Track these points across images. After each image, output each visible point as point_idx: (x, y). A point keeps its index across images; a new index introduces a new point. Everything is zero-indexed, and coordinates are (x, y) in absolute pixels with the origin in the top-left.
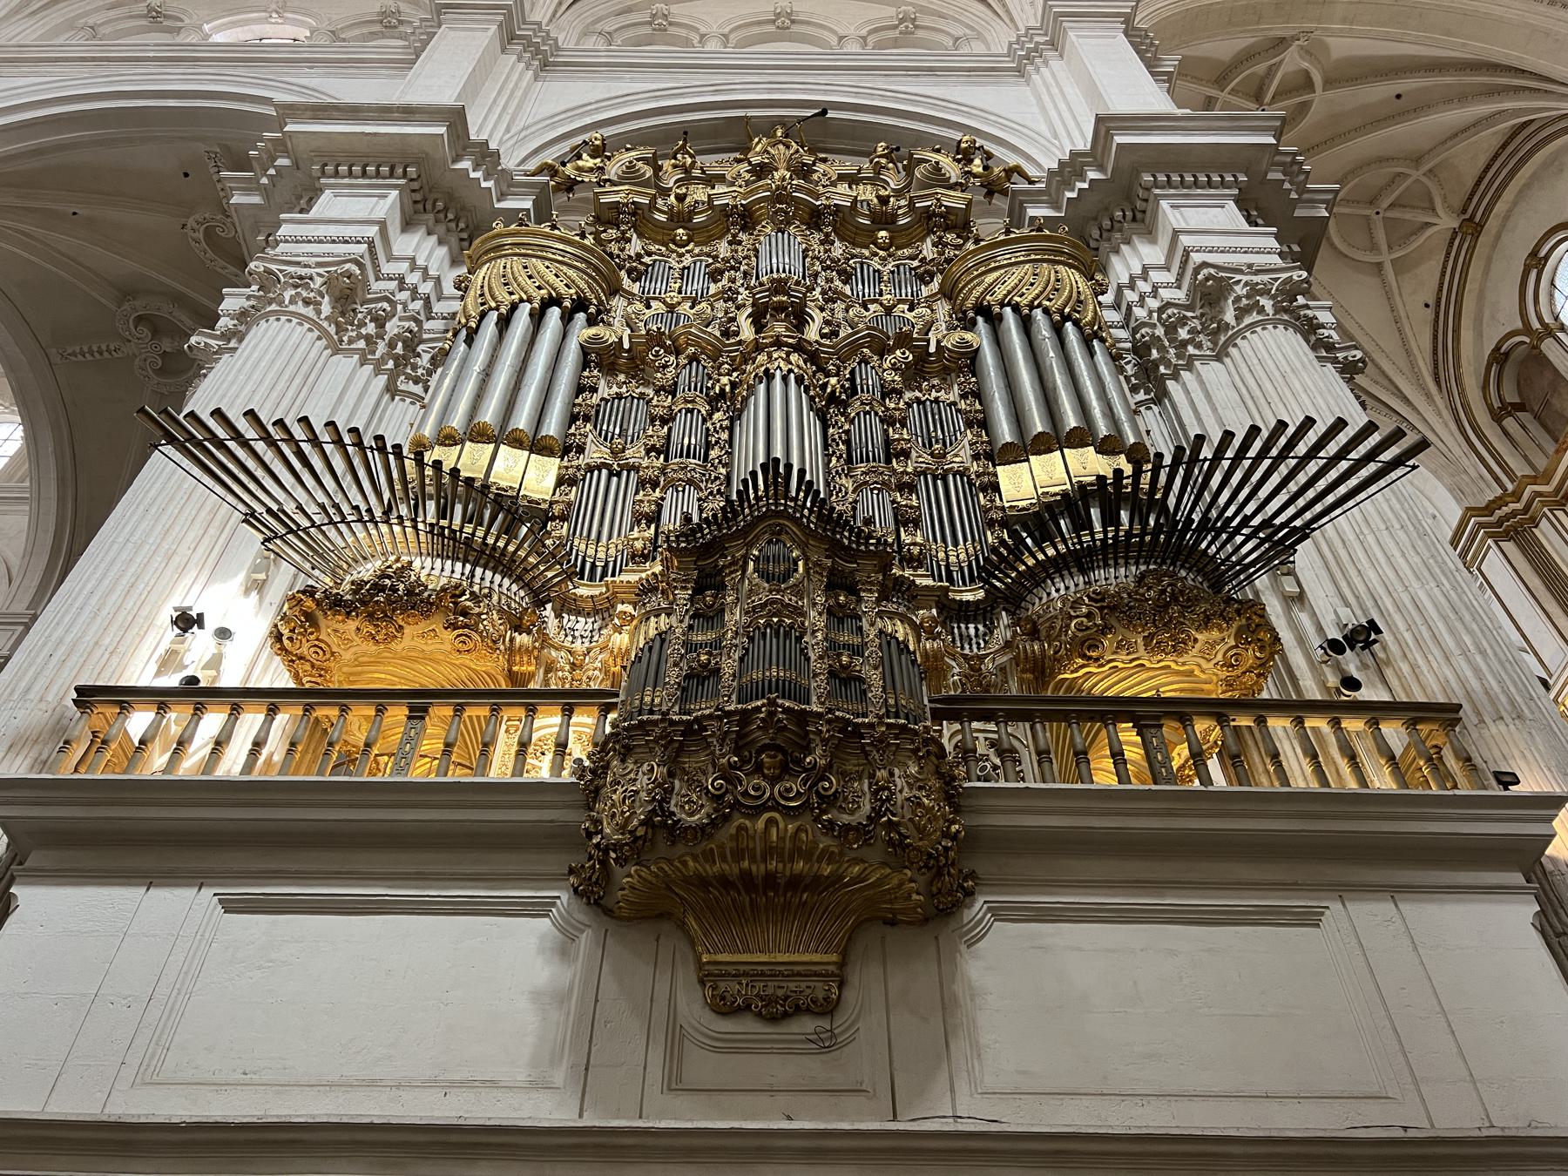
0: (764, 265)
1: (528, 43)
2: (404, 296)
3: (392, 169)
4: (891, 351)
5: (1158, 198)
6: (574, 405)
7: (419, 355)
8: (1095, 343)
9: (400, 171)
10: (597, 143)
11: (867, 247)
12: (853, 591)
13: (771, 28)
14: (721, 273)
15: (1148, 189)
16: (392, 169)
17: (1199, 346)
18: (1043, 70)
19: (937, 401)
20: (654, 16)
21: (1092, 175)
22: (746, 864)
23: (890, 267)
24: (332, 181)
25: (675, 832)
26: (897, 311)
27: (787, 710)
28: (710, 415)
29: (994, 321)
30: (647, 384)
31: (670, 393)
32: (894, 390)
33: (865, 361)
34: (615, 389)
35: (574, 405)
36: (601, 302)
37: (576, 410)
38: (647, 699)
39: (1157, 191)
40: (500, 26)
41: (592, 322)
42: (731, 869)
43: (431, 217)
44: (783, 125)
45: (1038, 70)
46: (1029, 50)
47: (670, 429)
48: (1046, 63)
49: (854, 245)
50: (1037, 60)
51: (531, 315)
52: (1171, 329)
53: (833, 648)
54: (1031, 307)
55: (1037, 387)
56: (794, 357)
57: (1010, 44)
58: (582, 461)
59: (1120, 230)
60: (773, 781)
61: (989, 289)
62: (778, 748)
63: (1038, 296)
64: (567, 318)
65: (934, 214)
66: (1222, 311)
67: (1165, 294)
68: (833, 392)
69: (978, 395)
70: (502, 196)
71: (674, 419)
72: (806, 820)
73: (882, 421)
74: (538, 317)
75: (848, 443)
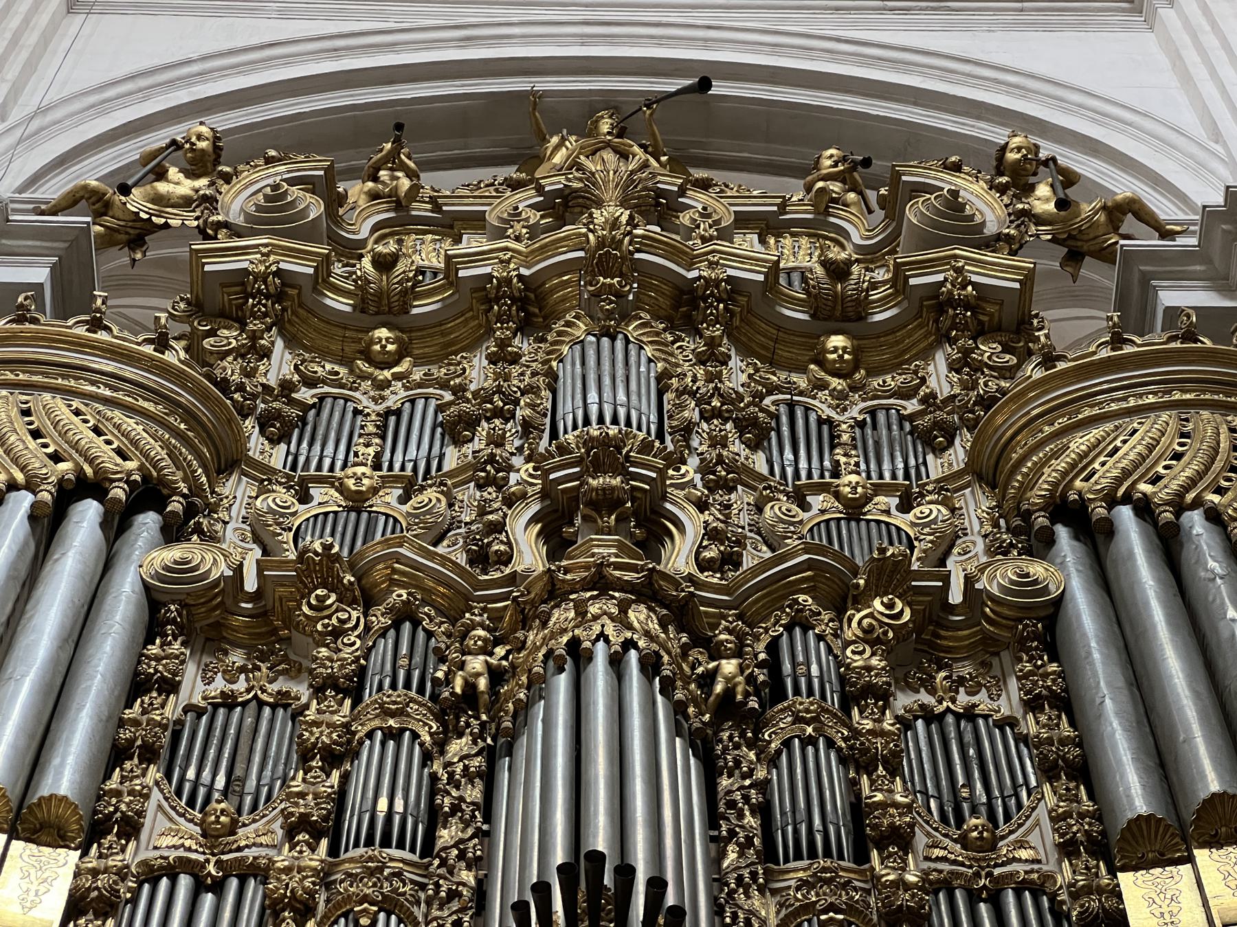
0: (568, 408)
4: (860, 599)
6: (122, 723)
10: (203, 145)
11: (803, 370)
14: (471, 423)
19: (970, 714)
23: (854, 412)
26: (872, 512)
28: (441, 745)
30: (294, 671)
31: (346, 692)
32: (870, 690)
34: (219, 684)
35: (122, 723)
36: (196, 489)
37: (125, 734)
41: (172, 533)
47: (345, 778)
49: (774, 363)
51: (33, 518)
54: (1179, 506)
55: (1203, 688)
56: (638, 615)
58: (132, 855)
61: (1081, 466)
63: (1193, 482)
65: (951, 302)
68: (729, 692)
71: (356, 755)
73: (842, 761)
75: (764, 811)
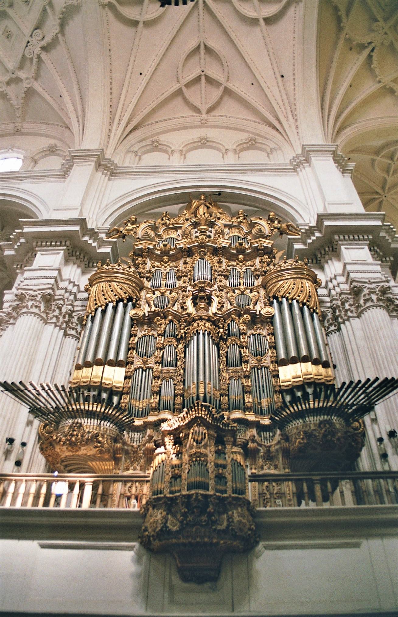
0: (196, 274)
1: (106, 167)
2: (67, 295)
3: (61, 243)
4: (242, 316)
6: (129, 344)
7: (73, 317)
8: (315, 314)
9: (63, 244)
10: (134, 220)
11: (235, 261)
13: (199, 144)
14: (181, 277)
15: (337, 242)
16: (61, 243)
17: (352, 312)
18: (303, 171)
19: (259, 334)
20: (153, 142)
21: (317, 234)
22: (190, 540)
23: (243, 270)
24: (40, 249)
25: (169, 532)
26: (245, 293)
27: (202, 495)
28: (177, 346)
29: (280, 304)
30: (154, 330)
31: (162, 336)
32: (243, 333)
33: (233, 320)
34: (143, 333)
35: (129, 344)
36: (137, 297)
37: (130, 346)
38: (159, 486)
39: (340, 242)
40: (96, 163)
41: (134, 306)
43: (75, 258)
45: (301, 170)
46: (298, 163)
47: (163, 352)
48: (304, 168)
49: (230, 260)
50: (301, 167)
52: (343, 304)
53: (217, 466)
54: (292, 299)
55: (293, 333)
56: (208, 324)
57: (291, 160)
58: (133, 367)
59: (328, 255)
61: (278, 290)
63: (295, 295)
64: (125, 306)
65: (259, 250)
66: (359, 299)
67: (342, 286)
68: (221, 335)
69: (273, 334)
70: (100, 247)
71: (165, 348)
73: (239, 347)
74: (115, 308)
75: (227, 357)
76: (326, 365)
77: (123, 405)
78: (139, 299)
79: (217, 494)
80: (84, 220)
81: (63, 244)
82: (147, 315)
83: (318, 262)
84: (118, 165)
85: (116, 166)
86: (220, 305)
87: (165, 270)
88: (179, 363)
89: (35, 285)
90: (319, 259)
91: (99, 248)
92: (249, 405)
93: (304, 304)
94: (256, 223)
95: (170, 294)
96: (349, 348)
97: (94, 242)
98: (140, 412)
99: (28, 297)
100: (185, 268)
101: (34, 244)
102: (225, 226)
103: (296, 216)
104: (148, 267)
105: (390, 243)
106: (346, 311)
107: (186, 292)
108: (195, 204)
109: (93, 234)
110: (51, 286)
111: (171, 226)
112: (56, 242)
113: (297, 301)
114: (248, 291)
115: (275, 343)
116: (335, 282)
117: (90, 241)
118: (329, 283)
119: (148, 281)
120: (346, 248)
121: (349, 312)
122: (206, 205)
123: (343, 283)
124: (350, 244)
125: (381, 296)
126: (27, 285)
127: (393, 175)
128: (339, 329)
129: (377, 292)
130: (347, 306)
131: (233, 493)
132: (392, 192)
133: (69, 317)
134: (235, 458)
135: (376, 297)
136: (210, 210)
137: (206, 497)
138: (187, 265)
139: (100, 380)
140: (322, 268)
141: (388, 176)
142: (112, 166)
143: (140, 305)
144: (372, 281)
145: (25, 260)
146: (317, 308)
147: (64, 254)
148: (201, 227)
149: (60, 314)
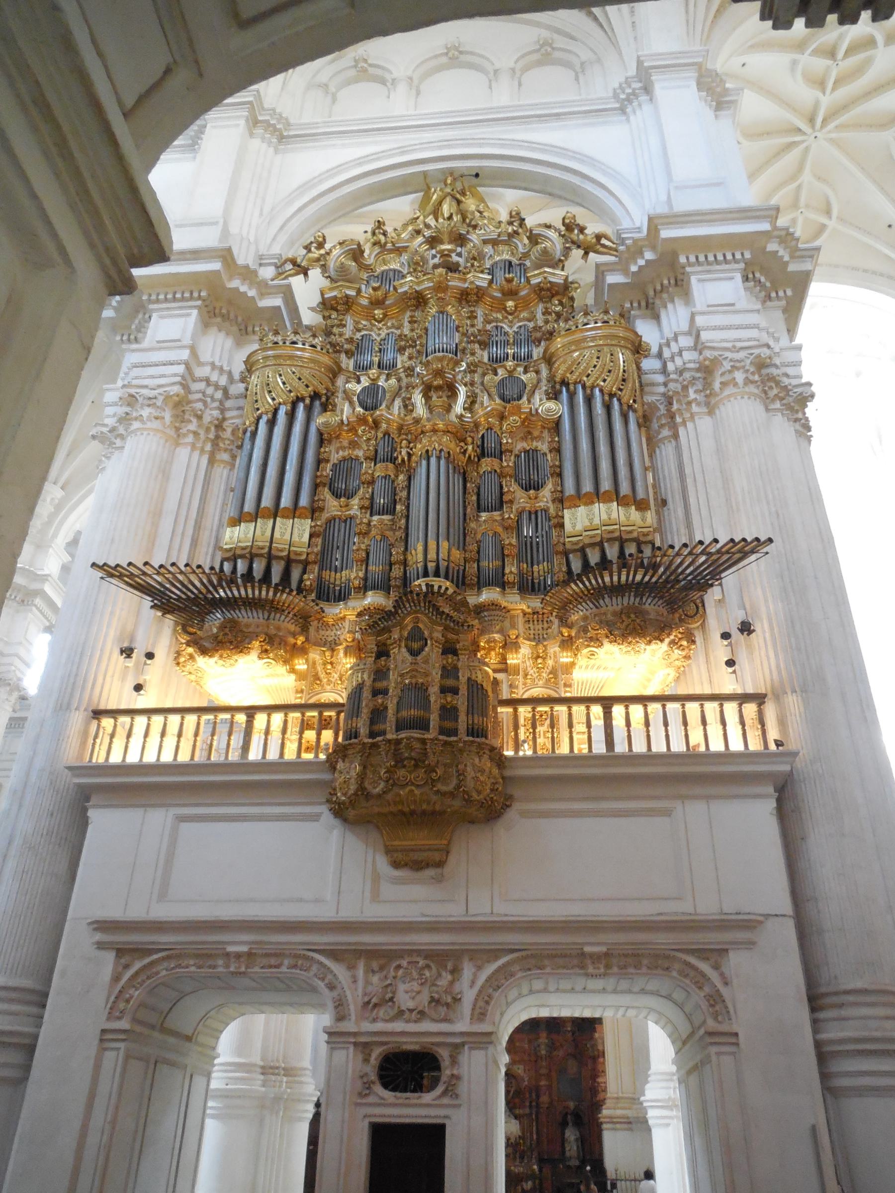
0: (430, 343)
1: (267, 125)
3: (191, 293)
5: (688, 275)
7: (224, 430)
8: (631, 414)
9: (196, 295)
10: (321, 239)
12: (455, 652)
15: (684, 268)
16: (191, 293)
17: (698, 404)
18: (638, 112)
20: (356, 61)
21: (649, 255)
23: (515, 329)
24: (155, 306)
25: (368, 796)
27: (418, 739)
29: (572, 396)
35: (317, 477)
36: (328, 389)
38: (354, 725)
39: (688, 269)
40: (247, 121)
41: (325, 408)
42: (393, 809)
44: (451, 174)
45: (634, 112)
46: (628, 95)
47: (373, 489)
48: (640, 105)
50: (635, 104)
51: (286, 413)
52: (685, 388)
53: (444, 690)
59: (668, 292)
60: (410, 772)
62: (411, 758)
63: (597, 378)
64: (309, 410)
68: (470, 457)
69: (558, 450)
70: (262, 295)
72: (426, 789)
73: (499, 477)
74: (291, 416)
75: (478, 495)
76: (642, 506)
77: (308, 583)
78: (333, 394)
79: (441, 737)
80: (229, 250)
81: (196, 295)
82: (346, 422)
83: (650, 306)
84: (292, 121)
85: (288, 124)
86: (469, 401)
87: (379, 335)
88: (398, 507)
89: (152, 377)
90: (651, 301)
91: (260, 300)
92: (511, 578)
93: (612, 395)
94: (540, 235)
95: (387, 380)
96: (688, 470)
97: (250, 289)
98: (337, 594)
99: (140, 399)
100: (412, 330)
101: (145, 297)
102: (485, 242)
103: (619, 212)
104: (348, 332)
105: (787, 263)
106: (689, 403)
107: (413, 376)
108: (435, 197)
109: (248, 274)
110: (178, 379)
111: (389, 246)
112: (183, 293)
113: (601, 391)
114: (520, 369)
115: (560, 467)
116: (674, 348)
117: (243, 289)
118: (665, 349)
119: (349, 358)
120: (699, 280)
121: (694, 405)
122: (454, 197)
123: (689, 349)
124: (709, 272)
125: (753, 373)
126: (136, 378)
127: (834, 89)
128: (676, 436)
129: (747, 368)
130: (692, 395)
131: (468, 735)
132: (831, 126)
133: (217, 431)
134: (473, 677)
135: (744, 376)
136: (462, 206)
137: (423, 741)
138: (416, 325)
139: (268, 544)
140: (657, 317)
141: (824, 93)
142: (279, 123)
143: (335, 406)
144: (739, 345)
145: (133, 327)
146: (634, 401)
147: (200, 314)
148: (443, 247)
149: (200, 426)
